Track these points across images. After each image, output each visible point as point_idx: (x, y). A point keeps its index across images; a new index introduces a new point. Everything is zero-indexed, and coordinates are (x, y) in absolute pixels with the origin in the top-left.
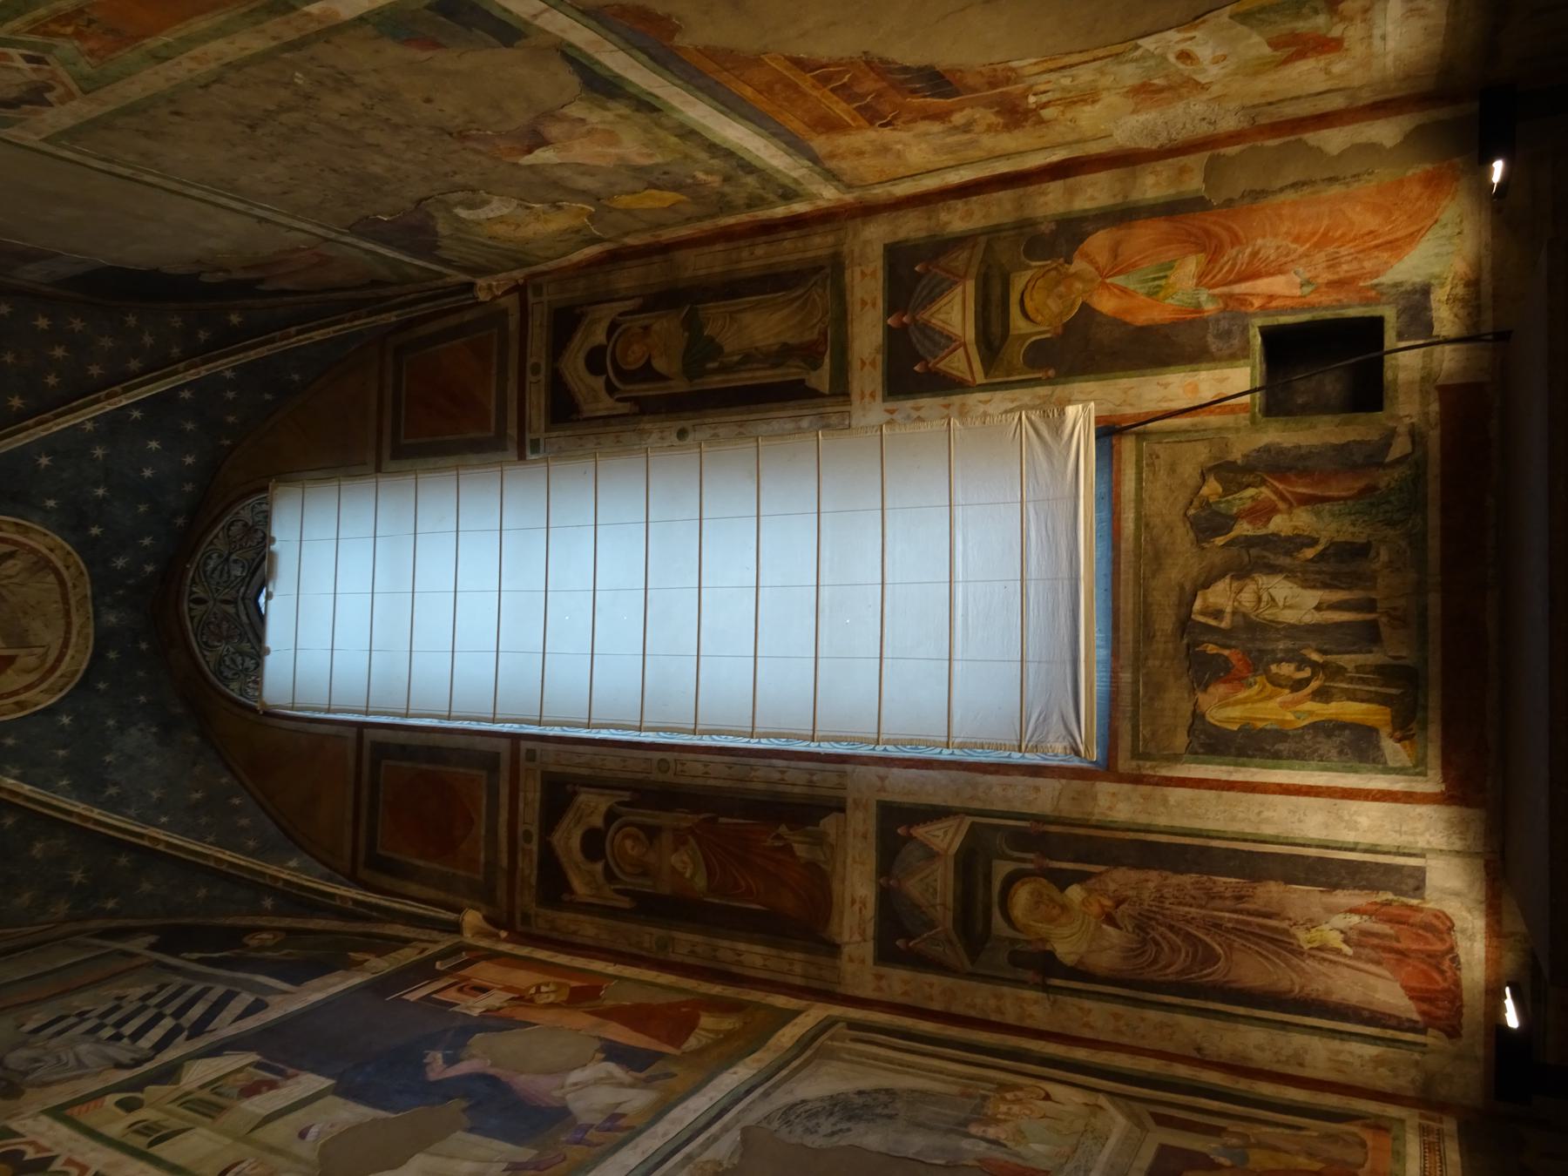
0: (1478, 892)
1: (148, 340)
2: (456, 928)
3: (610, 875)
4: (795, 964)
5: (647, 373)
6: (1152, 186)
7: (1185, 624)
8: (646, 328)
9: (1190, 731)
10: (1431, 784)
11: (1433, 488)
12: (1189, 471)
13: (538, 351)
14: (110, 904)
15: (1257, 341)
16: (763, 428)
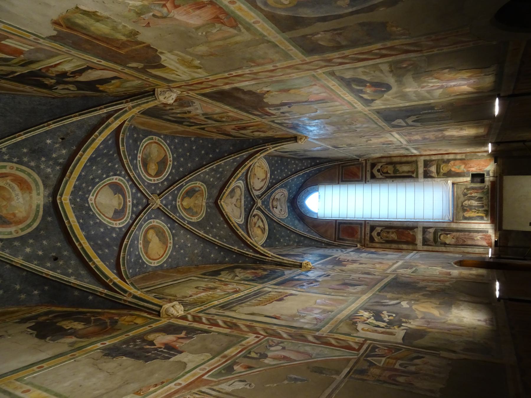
0: (494, 232)
1: (305, 164)
2: (357, 246)
3: (381, 238)
4: (411, 247)
5: (387, 173)
6: (459, 157)
7: (462, 205)
10: (489, 222)
11: (490, 191)
12: (463, 189)
13: (369, 168)
15: (471, 175)
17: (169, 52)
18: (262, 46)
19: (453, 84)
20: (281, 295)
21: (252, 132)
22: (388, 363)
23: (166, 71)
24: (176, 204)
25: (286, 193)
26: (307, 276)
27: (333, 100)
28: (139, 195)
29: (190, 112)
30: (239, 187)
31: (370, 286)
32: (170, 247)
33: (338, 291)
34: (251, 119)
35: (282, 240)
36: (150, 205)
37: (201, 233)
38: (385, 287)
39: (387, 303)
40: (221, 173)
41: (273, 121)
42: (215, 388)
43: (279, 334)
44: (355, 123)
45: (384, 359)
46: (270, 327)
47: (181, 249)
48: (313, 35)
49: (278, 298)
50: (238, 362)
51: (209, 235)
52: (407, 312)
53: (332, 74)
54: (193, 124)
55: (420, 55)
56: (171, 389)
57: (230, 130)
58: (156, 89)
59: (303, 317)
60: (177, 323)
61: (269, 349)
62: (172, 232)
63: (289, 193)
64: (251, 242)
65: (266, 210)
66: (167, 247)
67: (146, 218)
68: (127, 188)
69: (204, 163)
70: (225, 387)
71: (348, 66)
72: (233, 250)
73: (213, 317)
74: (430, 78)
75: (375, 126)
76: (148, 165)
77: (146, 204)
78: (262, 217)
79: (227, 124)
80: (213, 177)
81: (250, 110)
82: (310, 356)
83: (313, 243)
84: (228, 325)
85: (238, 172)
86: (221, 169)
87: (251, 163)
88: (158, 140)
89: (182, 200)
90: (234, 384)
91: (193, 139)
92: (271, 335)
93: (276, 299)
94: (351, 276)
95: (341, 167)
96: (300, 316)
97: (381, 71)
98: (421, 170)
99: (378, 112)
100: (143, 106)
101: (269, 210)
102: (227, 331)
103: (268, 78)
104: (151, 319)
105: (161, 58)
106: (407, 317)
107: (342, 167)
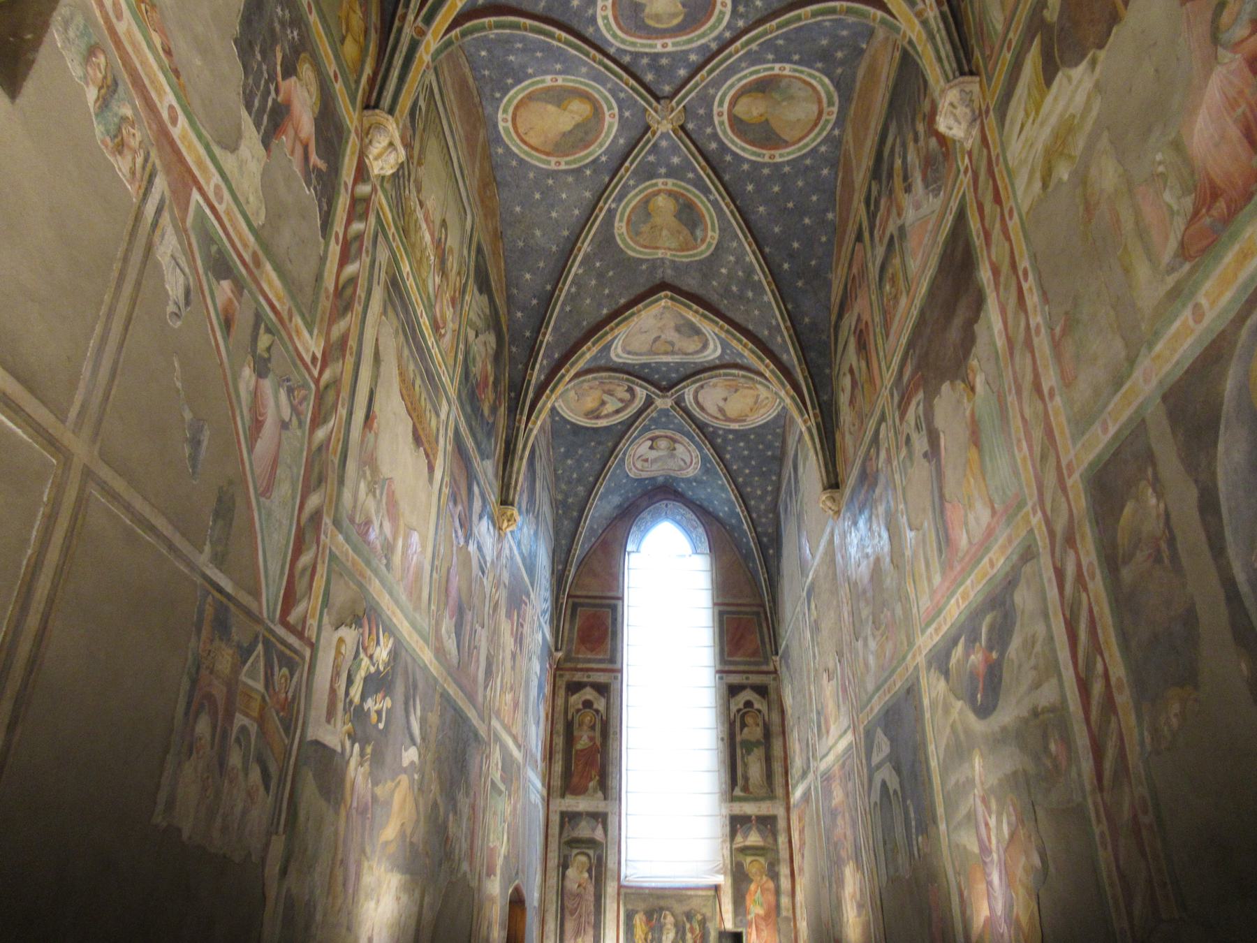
1: (764, 520)
2: (557, 650)
3: (578, 711)
4: (557, 782)
5: (743, 725)
6: (785, 901)
7: (661, 909)
8: (758, 725)
9: (633, 910)
12: (704, 910)
13: (755, 679)
14: (560, 512)
15: (739, 930)
16: (722, 770)
17: (1097, 86)
18: (1119, 344)
19: (996, 878)
20: (429, 442)
21: (851, 371)
22: (251, 697)
23: (1035, 92)
24: (660, 176)
25: (691, 472)
26: (481, 518)
27: (946, 567)
28: (682, 72)
29: (908, 189)
30: (705, 346)
31: (459, 672)
32: (549, 163)
33: (443, 589)
34: (889, 358)
35: (569, 462)
36: (655, 103)
37: (586, 244)
38: (455, 710)
39: (412, 710)
40: (741, 297)
41: (883, 418)
42: (166, 218)
43: (325, 421)
44: (878, 633)
45: (260, 686)
46: (344, 399)
47: (542, 193)
48: (1156, 483)
49: (421, 432)
50: (241, 294)
51: (579, 267)
52: (389, 759)
53: (1028, 554)
54: (872, 207)
55: (1088, 787)
56: (160, 93)
57: (856, 311)
58: (977, 79)
59: (371, 491)
60: (348, 152)
61: (280, 385)
62: (586, 166)
63: (688, 481)
64: (563, 376)
65: (646, 422)
66: (548, 154)
67: (622, 95)
68: (700, 37)
69: (767, 250)
70: (168, 246)
71: (1053, 593)
72: (543, 330)
73: (367, 252)
74: (1013, 818)
75: (870, 687)
76: (760, 95)
77: (658, 93)
78: (629, 410)
79: (873, 297)
80: (730, 276)
81: (917, 352)
82: (267, 491)
83: (563, 542)
84: (344, 287)
85: (745, 340)
86: (750, 294)
87: (768, 374)
88: (827, 121)
89: (670, 193)
90: (178, 270)
91: (830, 216)
92: (320, 397)
93: (418, 426)
94: (483, 627)
95: (755, 609)
96: (375, 483)
97: (1037, 685)
98: (750, 809)
99: (911, 692)
100: (929, 47)
101: (646, 429)
102: (329, 283)
103: (1016, 380)
104: (358, 82)
105: (1076, 65)
106: (377, 760)
107: (758, 614)
